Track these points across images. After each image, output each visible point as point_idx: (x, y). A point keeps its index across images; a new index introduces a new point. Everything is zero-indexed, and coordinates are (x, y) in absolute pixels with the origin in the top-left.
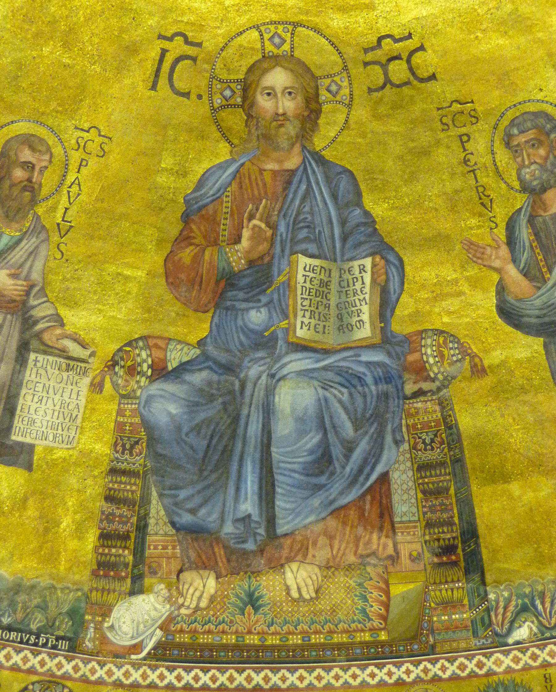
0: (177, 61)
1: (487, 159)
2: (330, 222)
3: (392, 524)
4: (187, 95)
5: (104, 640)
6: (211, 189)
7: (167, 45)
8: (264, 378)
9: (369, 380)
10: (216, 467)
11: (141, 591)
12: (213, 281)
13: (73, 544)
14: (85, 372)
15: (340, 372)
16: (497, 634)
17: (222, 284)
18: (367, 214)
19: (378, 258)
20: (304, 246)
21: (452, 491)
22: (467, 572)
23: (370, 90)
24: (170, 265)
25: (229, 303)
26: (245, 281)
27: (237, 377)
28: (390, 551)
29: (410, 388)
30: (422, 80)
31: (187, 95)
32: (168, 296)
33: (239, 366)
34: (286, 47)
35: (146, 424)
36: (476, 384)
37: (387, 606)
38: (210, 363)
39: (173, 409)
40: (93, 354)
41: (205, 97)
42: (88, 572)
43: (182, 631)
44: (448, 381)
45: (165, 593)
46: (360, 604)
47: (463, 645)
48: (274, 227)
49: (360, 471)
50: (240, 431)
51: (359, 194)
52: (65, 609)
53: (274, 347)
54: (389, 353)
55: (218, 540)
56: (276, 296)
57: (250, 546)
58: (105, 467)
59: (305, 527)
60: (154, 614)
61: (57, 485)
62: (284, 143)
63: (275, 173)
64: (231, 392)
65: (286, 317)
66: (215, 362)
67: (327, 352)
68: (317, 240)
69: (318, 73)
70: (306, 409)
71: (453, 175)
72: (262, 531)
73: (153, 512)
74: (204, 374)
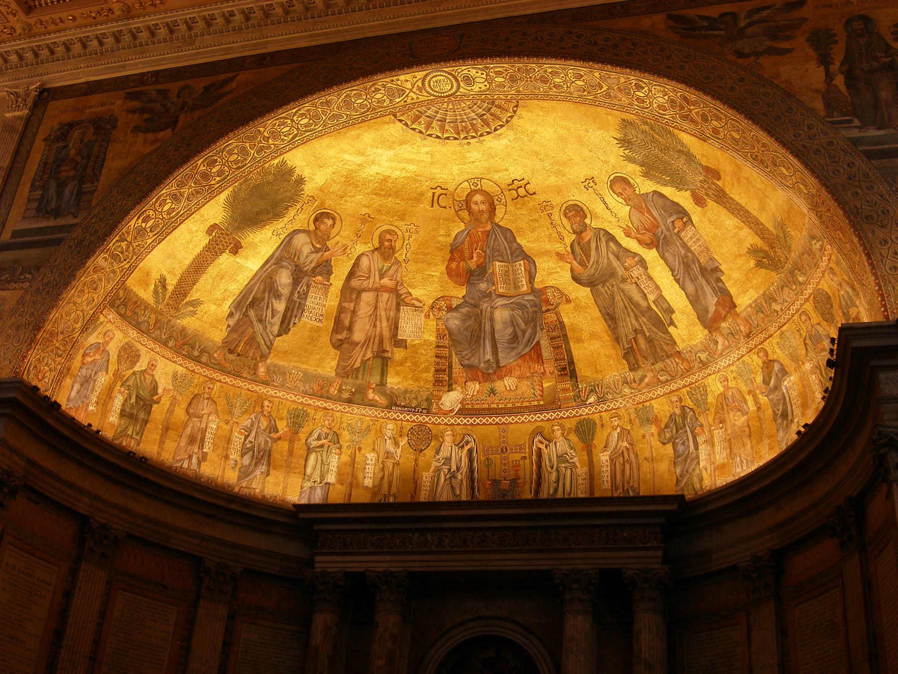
0: (440, 195)
2: (506, 248)
3: (542, 360)
4: (445, 207)
6: (459, 240)
7: (434, 191)
8: (489, 308)
9: (529, 306)
10: (475, 342)
12: (465, 275)
15: (517, 304)
16: (583, 401)
17: (468, 275)
19: (525, 261)
20: (497, 258)
21: (564, 347)
22: (571, 377)
23: (513, 199)
24: (448, 270)
25: (472, 282)
26: (477, 273)
27: (479, 309)
29: (544, 309)
30: (531, 195)
31: (445, 207)
34: (479, 186)
35: (447, 328)
36: (568, 306)
38: (468, 304)
39: (457, 322)
40: (424, 305)
41: (452, 207)
42: (431, 384)
43: (468, 404)
44: (558, 305)
46: (533, 391)
47: (571, 405)
48: (485, 252)
49: (529, 341)
50: (483, 329)
53: (491, 296)
54: (535, 296)
55: (479, 369)
56: (489, 278)
57: (491, 371)
59: (510, 363)
60: (457, 398)
61: (417, 353)
62: (484, 221)
64: (477, 315)
65: (494, 285)
66: (472, 305)
67: (511, 297)
68: (502, 256)
69: (492, 195)
70: (506, 319)
71: (548, 228)
72: (494, 366)
74: (466, 308)
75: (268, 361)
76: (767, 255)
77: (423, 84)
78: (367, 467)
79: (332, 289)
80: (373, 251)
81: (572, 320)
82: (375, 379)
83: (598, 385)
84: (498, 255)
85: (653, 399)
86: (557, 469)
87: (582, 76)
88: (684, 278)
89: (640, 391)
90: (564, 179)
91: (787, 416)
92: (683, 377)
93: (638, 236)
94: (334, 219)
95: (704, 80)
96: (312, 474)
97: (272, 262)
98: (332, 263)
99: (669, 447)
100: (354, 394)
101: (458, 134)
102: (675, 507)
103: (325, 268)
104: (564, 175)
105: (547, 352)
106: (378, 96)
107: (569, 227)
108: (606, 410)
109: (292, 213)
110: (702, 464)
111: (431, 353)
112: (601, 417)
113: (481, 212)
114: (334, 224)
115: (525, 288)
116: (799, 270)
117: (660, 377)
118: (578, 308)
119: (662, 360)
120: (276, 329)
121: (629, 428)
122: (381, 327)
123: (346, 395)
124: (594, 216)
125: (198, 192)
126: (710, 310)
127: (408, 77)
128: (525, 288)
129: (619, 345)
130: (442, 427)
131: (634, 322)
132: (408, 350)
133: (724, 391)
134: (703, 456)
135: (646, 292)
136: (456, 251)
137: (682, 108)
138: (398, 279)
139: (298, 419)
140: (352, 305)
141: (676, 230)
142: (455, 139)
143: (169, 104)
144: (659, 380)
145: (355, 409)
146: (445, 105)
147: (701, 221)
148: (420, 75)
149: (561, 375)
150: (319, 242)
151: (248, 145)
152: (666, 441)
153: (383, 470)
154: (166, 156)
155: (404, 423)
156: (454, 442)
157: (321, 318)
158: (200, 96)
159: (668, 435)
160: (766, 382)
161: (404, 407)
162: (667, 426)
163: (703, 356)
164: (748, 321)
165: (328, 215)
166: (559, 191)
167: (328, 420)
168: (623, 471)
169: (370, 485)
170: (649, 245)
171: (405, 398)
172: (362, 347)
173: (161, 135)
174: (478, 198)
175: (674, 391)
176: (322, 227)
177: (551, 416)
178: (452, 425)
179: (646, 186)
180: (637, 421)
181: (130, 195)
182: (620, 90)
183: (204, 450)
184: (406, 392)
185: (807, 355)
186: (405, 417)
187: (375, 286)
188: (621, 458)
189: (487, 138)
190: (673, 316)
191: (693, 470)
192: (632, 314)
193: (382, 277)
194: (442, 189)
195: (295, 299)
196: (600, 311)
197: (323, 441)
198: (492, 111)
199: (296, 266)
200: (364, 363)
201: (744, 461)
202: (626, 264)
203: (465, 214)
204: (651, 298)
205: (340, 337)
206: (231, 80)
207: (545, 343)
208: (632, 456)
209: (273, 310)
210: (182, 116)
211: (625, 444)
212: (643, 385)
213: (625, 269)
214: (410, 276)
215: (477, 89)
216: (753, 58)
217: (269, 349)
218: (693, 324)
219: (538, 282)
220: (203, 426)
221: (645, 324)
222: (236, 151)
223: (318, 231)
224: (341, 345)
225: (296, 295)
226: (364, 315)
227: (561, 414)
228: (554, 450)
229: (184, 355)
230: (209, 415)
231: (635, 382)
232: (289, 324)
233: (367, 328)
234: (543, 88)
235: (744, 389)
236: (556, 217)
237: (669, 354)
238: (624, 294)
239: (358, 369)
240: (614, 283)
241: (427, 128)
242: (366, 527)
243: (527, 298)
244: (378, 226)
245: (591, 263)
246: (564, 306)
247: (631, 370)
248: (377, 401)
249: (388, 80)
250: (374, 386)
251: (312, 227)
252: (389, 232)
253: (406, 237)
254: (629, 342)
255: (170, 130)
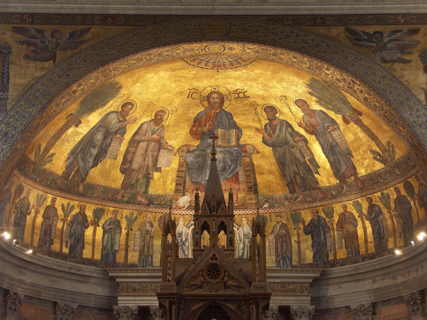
1: (260, 113)
4: (195, 99)
5: (177, 206)
6: (200, 116)
7: (190, 90)
9: (234, 153)
11: (185, 195)
13: (170, 187)
14: (172, 152)
15: (228, 151)
18: (234, 121)
22: (255, 193)
28: (238, 188)
29: (243, 155)
32: (191, 137)
33: (206, 150)
34: (217, 90)
35: (185, 161)
37: (237, 199)
39: (191, 159)
44: (252, 154)
45: (190, 195)
49: (232, 171)
51: (233, 118)
52: (169, 200)
54: (239, 148)
55: (201, 184)
58: (177, 170)
62: (216, 107)
63: (214, 113)
64: (204, 155)
67: (225, 147)
68: (223, 126)
69: (224, 95)
71: (253, 115)
73: (187, 179)
74: (198, 152)
75: (85, 182)
76: (379, 155)
77: (205, 48)
78: (136, 239)
79: (124, 141)
80: (150, 121)
81: (258, 162)
82: (143, 190)
83: (270, 199)
84: (220, 126)
85: (302, 209)
86: (244, 242)
87: (297, 58)
88: (329, 153)
89: (294, 204)
90: (268, 93)
91: (380, 234)
92: (320, 201)
93: (306, 128)
94: (133, 105)
95: (364, 75)
96: (106, 246)
97: (95, 129)
98: (127, 128)
99: (309, 237)
100: (130, 198)
101: (214, 67)
102: (318, 275)
103: (122, 131)
104: (268, 92)
105: (242, 178)
106: (178, 51)
107: (266, 117)
108: (274, 212)
109: (111, 103)
110: (328, 248)
111: (174, 175)
112: (270, 215)
113: (215, 103)
114: (132, 107)
115: (234, 143)
116: (398, 168)
117: (307, 199)
118: (263, 156)
119: (309, 190)
120: (91, 164)
121: (286, 223)
122: (148, 161)
123: (126, 199)
124: (281, 113)
125: (68, 100)
126: (342, 170)
127: (198, 45)
128: (234, 143)
129: (285, 179)
130: (177, 216)
131: (295, 168)
132: (162, 173)
133: (344, 212)
134: (329, 244)
135: (305, 155)
136: (197, 121)
137: (349, 83)
138: (162, 135)
139: (98, 214)
140: (134, 149)
141: (329, 130)
142: (211, 69)
143: (47, 43)
144: (306, 200)
145: (130, 206)
146: (213, 56)
147: (344, 130)
148: (205, 45)
149: (249, 191)
150: (122, 117)
151: (100, 75)
152: (307, 233)
153: (144, 240)
154: (53, 81)
155: (157, 214)
156: (184, 225)
157: (116, 157)
158: (68, 39)
159: (309, 230)
160: (370, 213)
161: (157, 205)
162: (308, 225)
163: (334, 193)
164: (363, 182)
165: (130, 103)
166: (263, 98)
167: (115, 214)
168: (282, 247)
169: (138, 250)
170: (311, 133)
171: (158, 200)
172: (137, 172)
173: (46, 64)
174: (215, 96)
175: (314, 207)
176: (126, 109)
177: (241, 212)
178: (184, 215)
179: (316, 107)
180: (291, 220)
181: (34, 105)
182: (316, 68)
183: (52, 238)
184: (159, 196)
185: (395, 208)
186: (157, 210)
187: (148, 139)
188: (281, 239)
189: (229, 70)
190: (318, 170)
191: (323, 251)
192: (294, 164)
193: (153, 134)
194: (195, 89)
195: (103, 147)
196: (276, 160)
197: (112, 226)
198: (238, 61)
199: (107, 130)
200: (137, 181)
201: (354, 251)
202: (296, 139)
203: (206, 103)
204: (307, 158)
205: (125, 167)
206: (87, 31)
207: (241, 173)
208: (288, 239)
209: (90, 154)
210: (58, 52)
211: (284, 232)
212: (296, 201)
213: (295, 142)
214: (169, 134)
215: (235, 52)
216: (390, 64)
217: (86, 176)
218: (331, 176)
219: (242, 141)
220: (51, 223)
221: (301, 170)
222: (94, 78)
223: (123, 112)
224: (125, 171)
225: (104, 145)
226: (139, 154)
227: (247, 212)
228: (242, 231)
229: (43, 185)
230: (53, 217)
231: (292, 199)
232: (98, 161)
233: (140, 161)
234: (272, 57)
235: (356, 214)
236: (259, 110)
237: (314, 187)
238: (292, 153)
239: (134, 184)
240: (287, 147)
241: (198, 64)
242: (147, 280)
243: (234, 148)
244: (155, 108)
245: (275, 135)
246: (255, 155)
247: (290, 192)
248: (142, 202)
249: (187, 45)
250: (141, 193)
251: (120, 110)
252: (161, 111)
253: (171, 113)
254: (291, 178)
255: (52, 61)
